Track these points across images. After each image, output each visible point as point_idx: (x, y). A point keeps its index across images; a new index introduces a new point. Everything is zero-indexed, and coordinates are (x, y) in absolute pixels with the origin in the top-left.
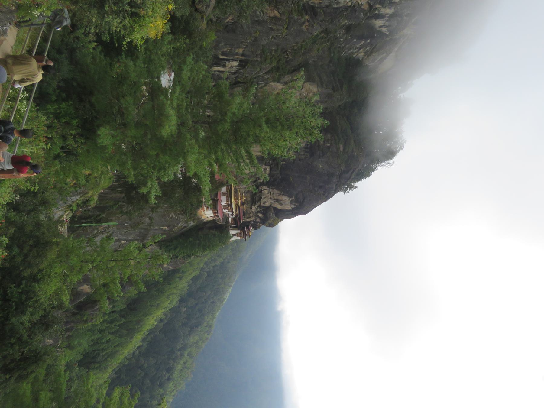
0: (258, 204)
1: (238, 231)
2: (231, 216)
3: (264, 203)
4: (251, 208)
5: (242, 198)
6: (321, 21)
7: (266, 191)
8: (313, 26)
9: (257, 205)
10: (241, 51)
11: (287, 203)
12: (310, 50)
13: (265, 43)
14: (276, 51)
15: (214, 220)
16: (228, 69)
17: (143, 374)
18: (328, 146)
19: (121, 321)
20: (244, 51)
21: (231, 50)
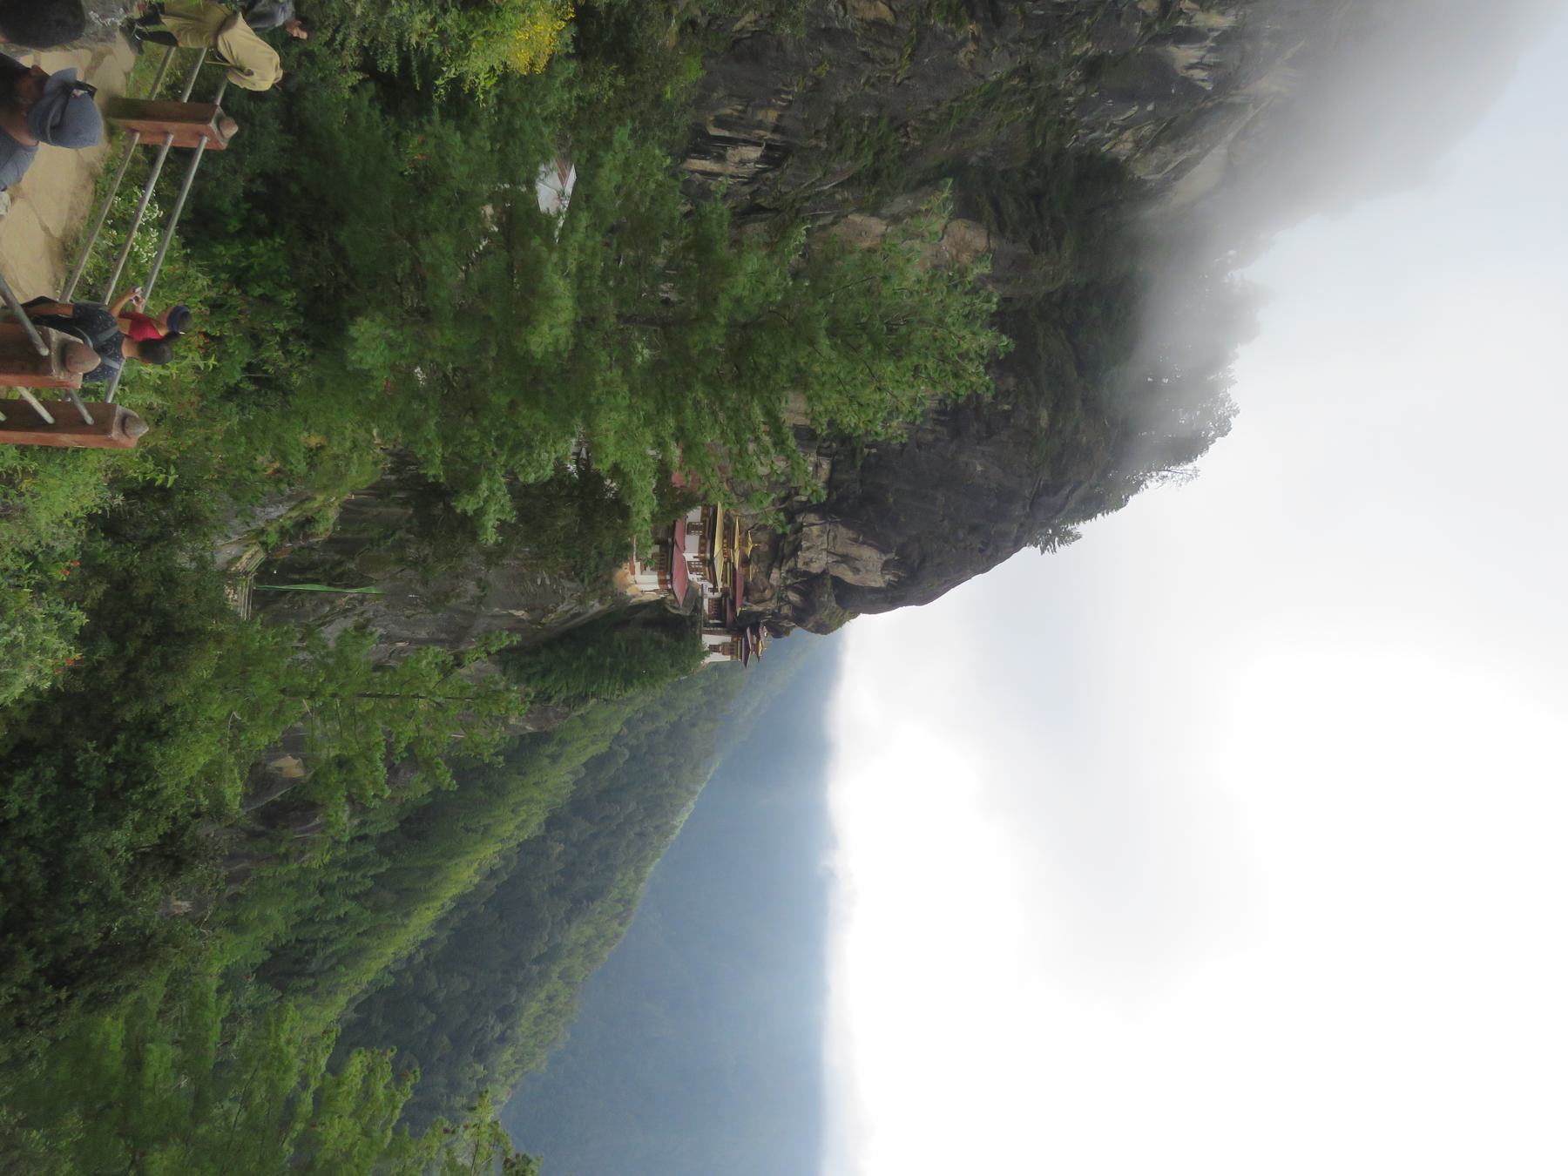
0: (791, 564)
1: (728, 639)
2: (710, 595)
3: (806, 564)
4: (768, 575)
5: (744, 543)
6: (1015, 41)
7: (815, 530)
8: (987, 54)
9: (785, 568)
10: (772, 116)
11: (871, 568)
12: (974, 124)
13: (843, 94)
14: (874, 122)
15: (660, 602)
16: (732, 169)
17: (433, 1017)
18: (1005, 411)
19: (380, 866)
20: (780, 117)
21: (744, 112)
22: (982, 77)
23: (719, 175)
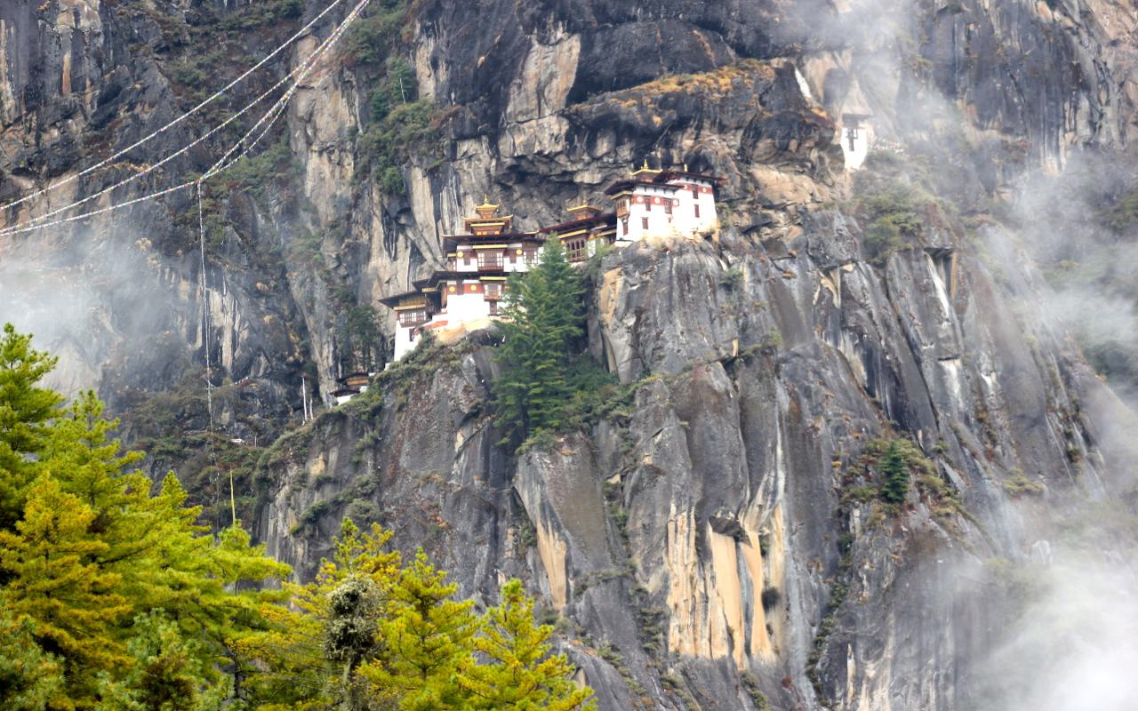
4: (592, 187)
20: (185, 278)
22: (164, 90)
23: (234, 332)
